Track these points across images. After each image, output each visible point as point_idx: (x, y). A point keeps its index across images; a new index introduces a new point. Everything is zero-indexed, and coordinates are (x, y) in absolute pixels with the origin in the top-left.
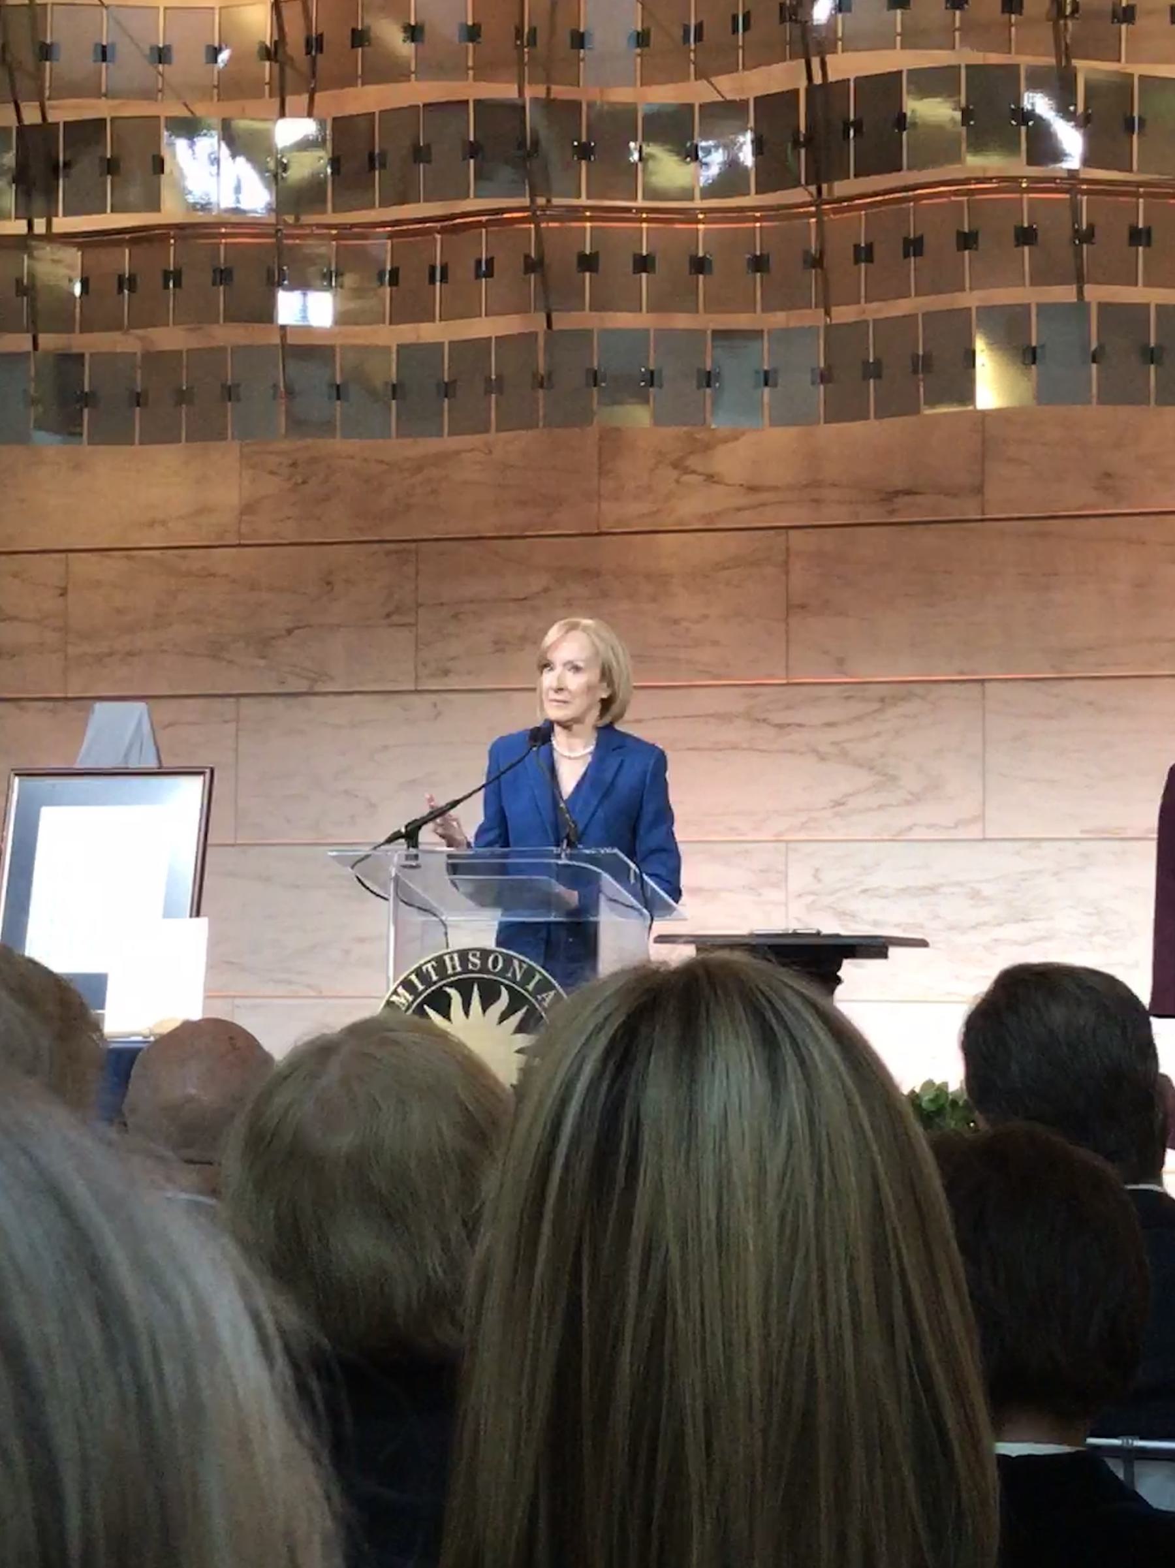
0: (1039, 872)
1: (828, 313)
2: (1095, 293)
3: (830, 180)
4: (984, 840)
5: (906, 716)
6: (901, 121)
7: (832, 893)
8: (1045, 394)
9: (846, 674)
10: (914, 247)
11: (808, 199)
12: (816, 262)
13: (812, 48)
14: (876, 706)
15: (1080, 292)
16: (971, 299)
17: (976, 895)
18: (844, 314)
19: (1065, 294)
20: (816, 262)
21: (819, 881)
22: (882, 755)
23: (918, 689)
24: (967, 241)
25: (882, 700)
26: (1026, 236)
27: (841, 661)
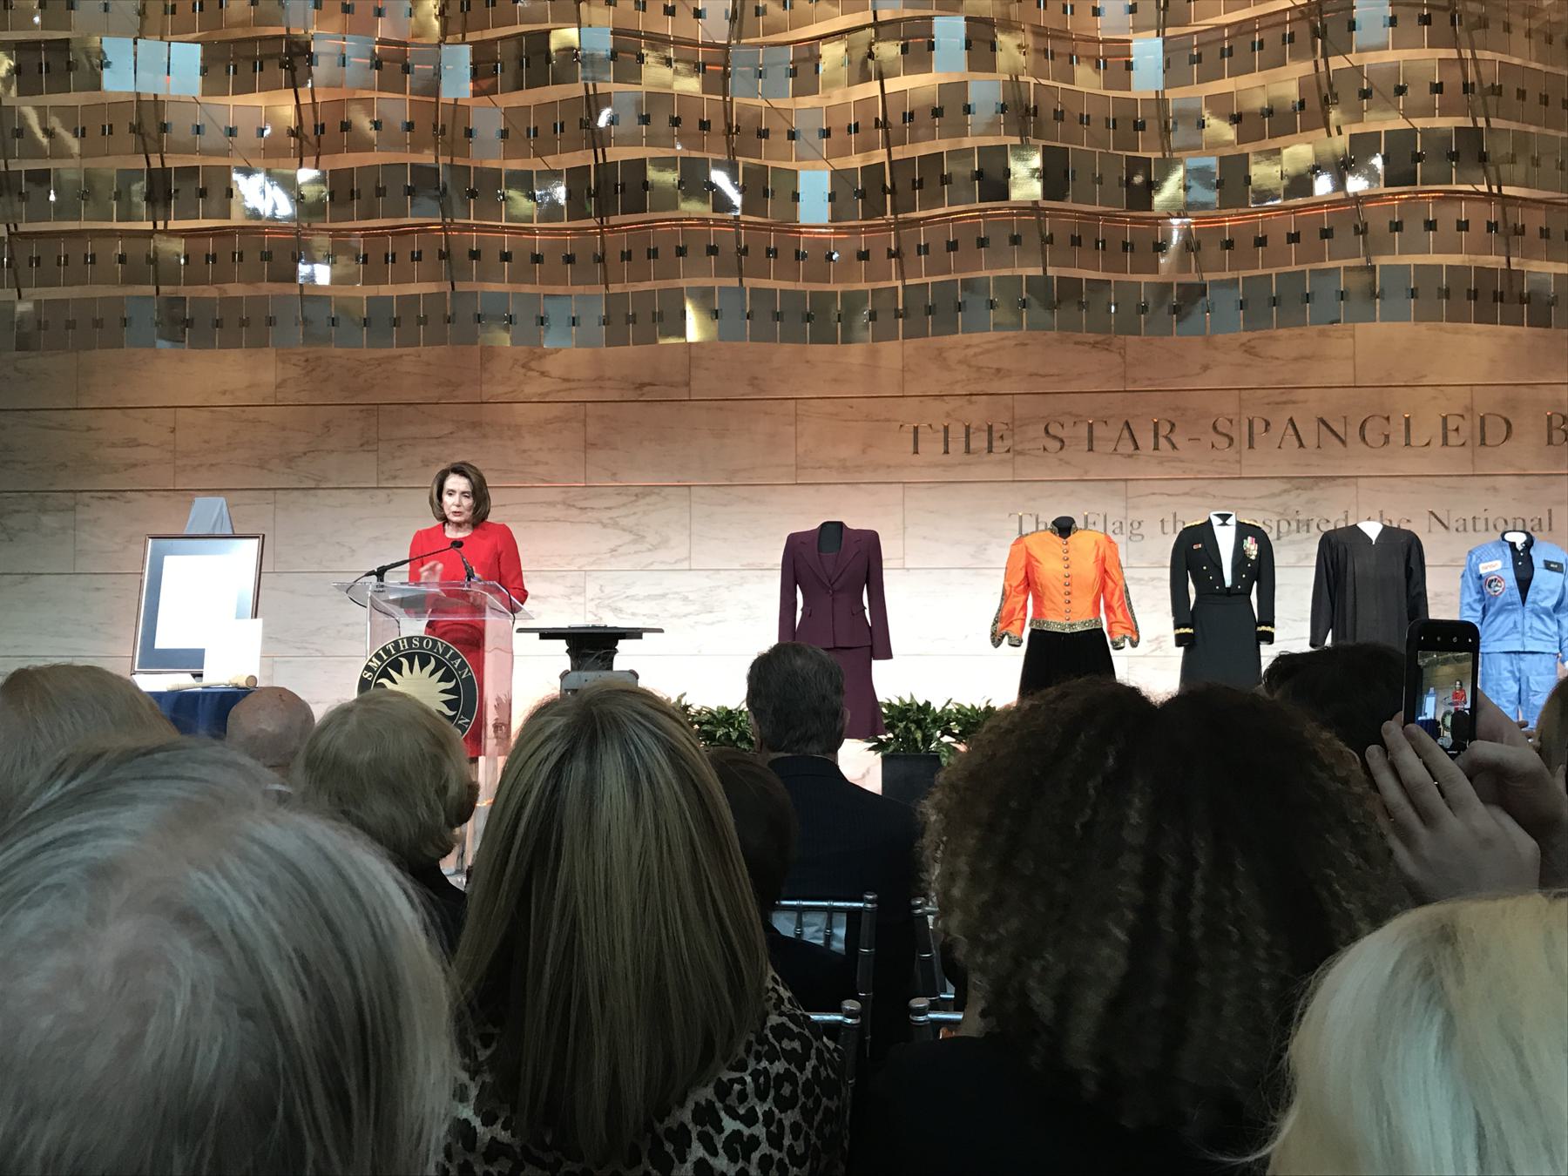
0: (719, 587)
1: (607, 287)
2: (749, 282)
3: (608, 216)
4: (690, 570)
5: (648, 504)
6: (646, 185)
7: (610, 598)
8: (722, 335)
9: (616, 481)
10: (653, 254)
11: (596, 225)
12: (601, 259)
13: (597, 142)
14: (634, 498)
15: (741, 281)
16: (682, 283)
17: (685, 599)
18: (616, 288)
19: (734, 282)
20: (601, 259)
21: (602, 592)
22: (637, 525)
23: (657, 490)
24: (681, 252)
25: (636, 495)
26: (712, 250)
27: (614, 474)
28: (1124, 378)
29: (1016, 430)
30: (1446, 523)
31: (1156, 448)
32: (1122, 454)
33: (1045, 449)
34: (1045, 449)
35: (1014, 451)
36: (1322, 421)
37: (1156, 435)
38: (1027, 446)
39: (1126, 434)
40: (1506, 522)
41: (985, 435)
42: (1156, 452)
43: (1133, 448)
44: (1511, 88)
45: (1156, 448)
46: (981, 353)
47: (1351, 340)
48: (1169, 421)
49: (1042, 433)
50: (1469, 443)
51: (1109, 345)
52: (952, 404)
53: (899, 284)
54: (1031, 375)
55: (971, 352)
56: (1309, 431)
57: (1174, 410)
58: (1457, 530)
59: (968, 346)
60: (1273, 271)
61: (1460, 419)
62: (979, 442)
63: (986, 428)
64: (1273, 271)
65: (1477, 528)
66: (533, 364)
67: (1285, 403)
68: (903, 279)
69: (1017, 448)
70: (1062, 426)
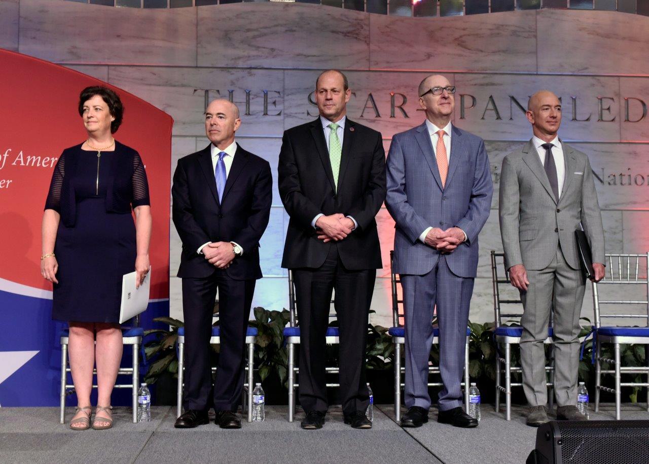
28: (369, 60)
29: (286, 98)
30: (601, 178)
31: (393, 116)
32: (367, 120)
33: (308, 114)
34: (308, 114)
35: (284, 114)
36: (513, 98)
37: (393, 106)
38: (293, 110)
39: (370, 104)
40: (643, 178)
41: (262, 100)
42: (393, 119)
43: (375, 115)
45: (393, 116)
46: (259, 36)
47: (535, 39)
48: (402, 95)
49: (306, 101)
50: (617, 119)
51: (357, 34)
54: (298, 55)
55: (251, 34)
56: (504, 107)
58: (609, 184)
59: (248, 30)
61: (611, 101)
62: (257, 106)
63: (262, 94)
65: (623, 183)
67: (487, 85)
69: (286, 112)
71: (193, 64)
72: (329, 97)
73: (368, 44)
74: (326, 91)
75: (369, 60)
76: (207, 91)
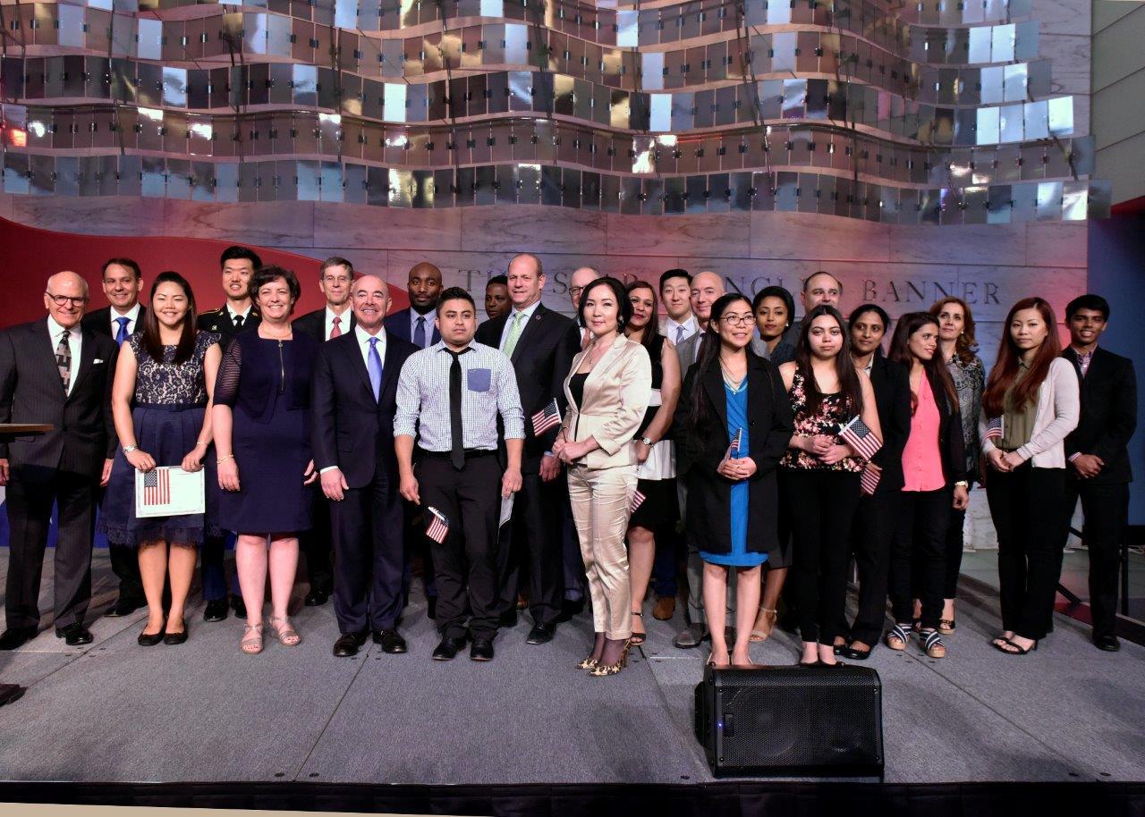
16: (294, 156)
28: (606, 246)
44: (863, 59)
46: (514, 225)
52: (495, 257)
53: (454, 167)
54: (547, 241)
55: (506, 223)
57: (637, 268)
59: (504, 220)
60: (707, 174)
64: (707, 174)
66: (202, 218)
68: (457, 164)
70: (566, 275)
71: (458, 249)
72: (518, 284)
73: (606, 232)
74: (516, 277)
75: (606, 246)
76: (469, 272)
